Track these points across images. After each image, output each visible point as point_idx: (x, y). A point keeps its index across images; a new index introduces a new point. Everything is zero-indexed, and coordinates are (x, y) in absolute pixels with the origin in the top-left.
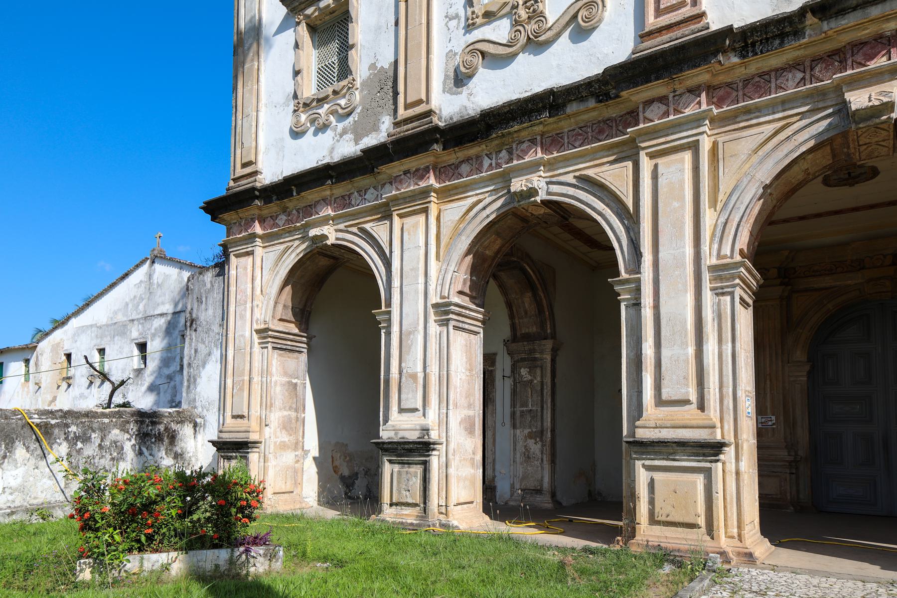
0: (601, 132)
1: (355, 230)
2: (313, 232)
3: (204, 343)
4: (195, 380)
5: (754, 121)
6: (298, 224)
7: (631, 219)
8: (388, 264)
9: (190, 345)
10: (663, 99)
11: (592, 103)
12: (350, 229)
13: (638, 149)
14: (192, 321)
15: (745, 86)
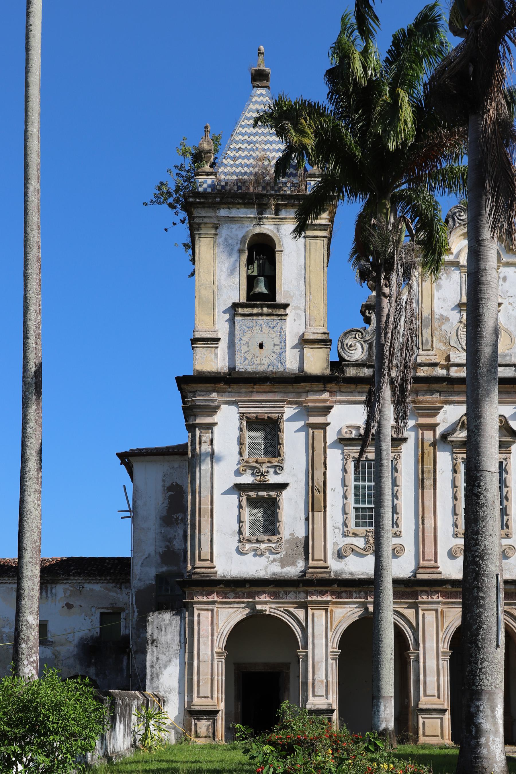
0: (403, 595)
1: (282, 609)
2: (259, 607)
3: (163, 653)
4: (158, 676)
5: (453, 606)
6: (246, 600)
7: (415, 631)
8: (304, 630)
9: (152, 655)
10: (426, 592)
11: (403, 586)
12: (279, 609)
13: (418, 607)
14: (153, 641)
15: (451, 594)
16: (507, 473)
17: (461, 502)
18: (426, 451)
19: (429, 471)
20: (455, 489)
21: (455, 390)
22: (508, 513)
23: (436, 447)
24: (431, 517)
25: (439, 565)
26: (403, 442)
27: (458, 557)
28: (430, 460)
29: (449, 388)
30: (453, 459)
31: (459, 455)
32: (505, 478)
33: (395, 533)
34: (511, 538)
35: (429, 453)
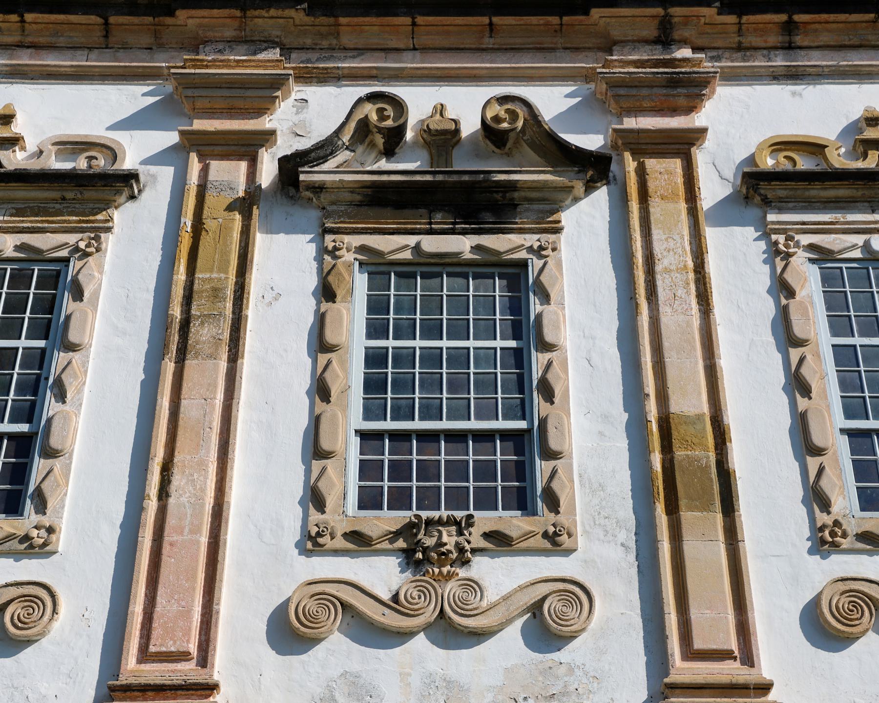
16: (545, 298)
17: (345, 408)
18: (210, 224)
19: (216, 293)
20: (323, 359)
21: (347, 40)
22: (553, 444)
23: (255, 211)
24: (202, 465)
25: (217, 675)
26: (119, 192)
27: (315, 641)
28: (225, 254)
29: (323, 36)
30: (323, 251)
31: (347, 238)
32: (539, 317)
33: (26, 538)
34: (569, 552)
35: (224, 230)
